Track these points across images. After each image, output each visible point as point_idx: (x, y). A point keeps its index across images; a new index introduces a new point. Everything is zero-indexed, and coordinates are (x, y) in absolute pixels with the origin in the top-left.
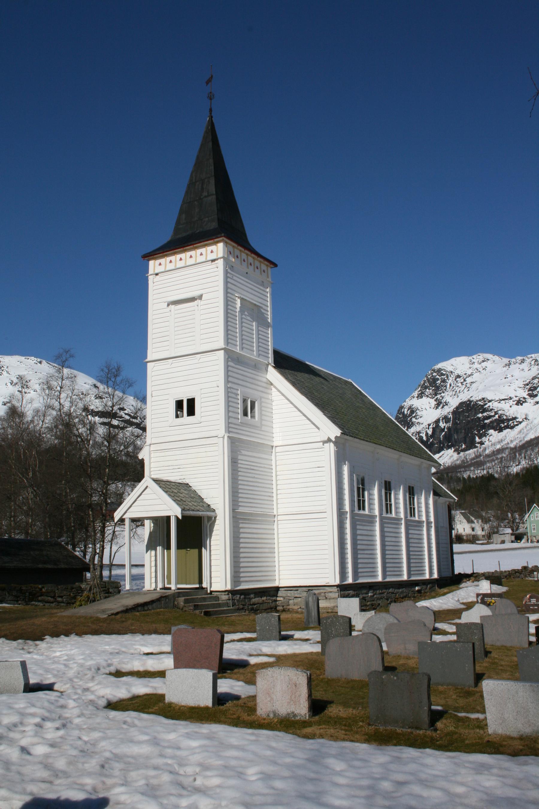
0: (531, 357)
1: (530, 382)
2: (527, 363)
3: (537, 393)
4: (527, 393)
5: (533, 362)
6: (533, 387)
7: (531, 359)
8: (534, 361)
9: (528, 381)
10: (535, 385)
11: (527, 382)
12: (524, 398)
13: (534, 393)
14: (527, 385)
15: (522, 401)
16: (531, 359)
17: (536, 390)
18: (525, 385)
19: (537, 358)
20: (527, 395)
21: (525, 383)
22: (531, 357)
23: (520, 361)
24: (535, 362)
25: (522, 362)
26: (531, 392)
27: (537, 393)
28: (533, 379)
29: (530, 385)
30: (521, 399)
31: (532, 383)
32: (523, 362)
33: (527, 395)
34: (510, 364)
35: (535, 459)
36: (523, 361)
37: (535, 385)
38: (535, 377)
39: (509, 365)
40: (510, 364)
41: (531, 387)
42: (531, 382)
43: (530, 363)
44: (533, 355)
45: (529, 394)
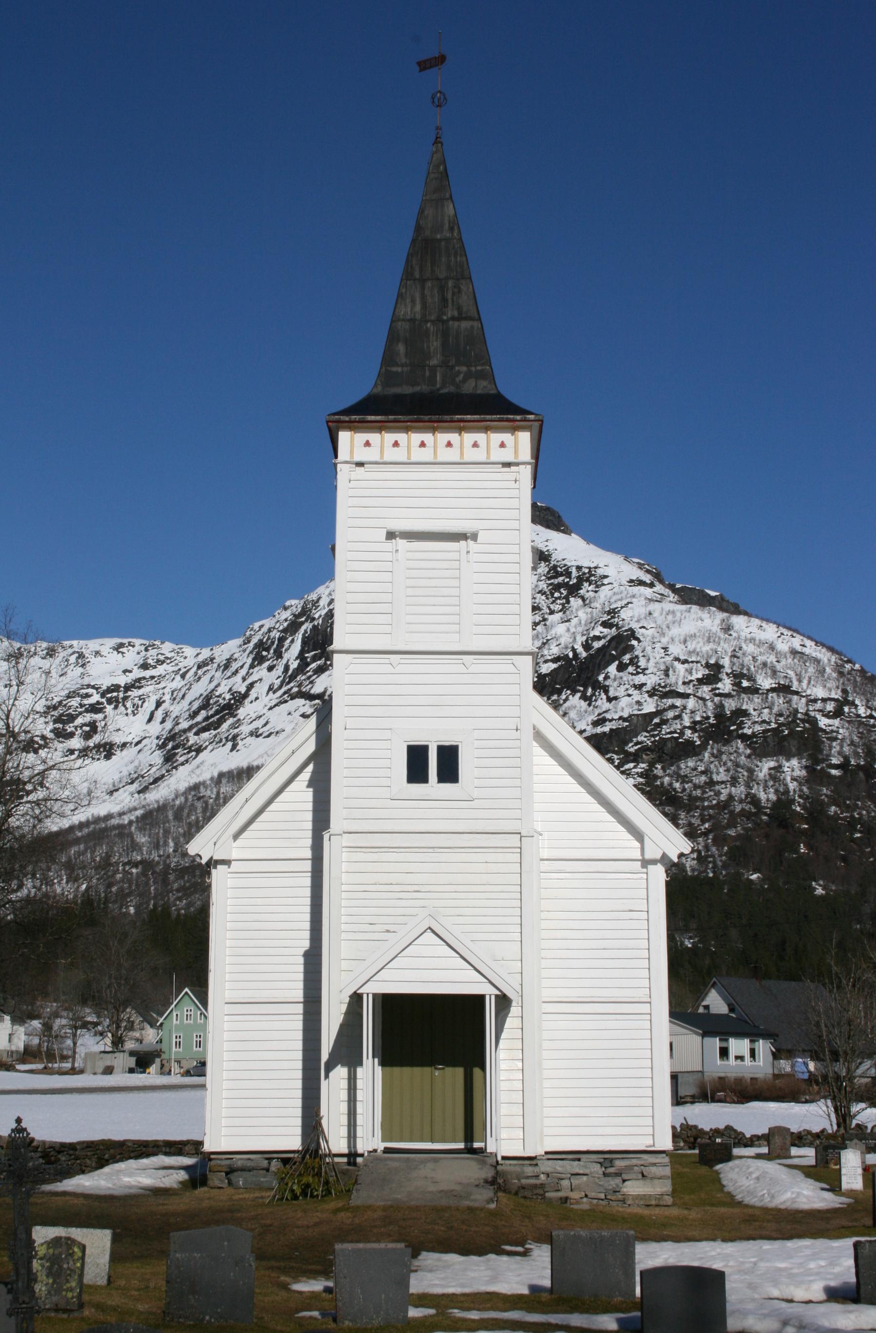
0: (71, 646)
1: (60, 702)
2: (60, 658)
3: (73, 729)
4: (51, 726)
5: (73, 659)
6: (68, 715)
7: (70, 651)
8: (77, 655)
9: (57, 700)
10: (70, 711)
11: (54, 702)
12: (43, 737)
13: (67, 728)
14: (55, 708)
15: (38, 743)
16: (70, 651)
17: (73, 722)
18: (48, 707)
19: (83, 650)
20: (51, 731)
21: (49, 703)
22: (71, 646)
23: (45, 652)
24: (78, 658)
25: (47, 654)
26: (61, 726)
27: (73, 729)
28: (68, 697)
29: (60, 710)
30: (36, 739)
31: (65, 706)
32: (51, 656)
33: (51, 731)
34: (21, 655)
35: (56, 881)
36: (51, 653)
37: (70, 711)
38: (74, 692)
39: (17, 658)
40: (21, 655)
41: (62, 715)
42: (64, 703)
43: (67, 660)
44: (75, 643)
45: (55, 729)
